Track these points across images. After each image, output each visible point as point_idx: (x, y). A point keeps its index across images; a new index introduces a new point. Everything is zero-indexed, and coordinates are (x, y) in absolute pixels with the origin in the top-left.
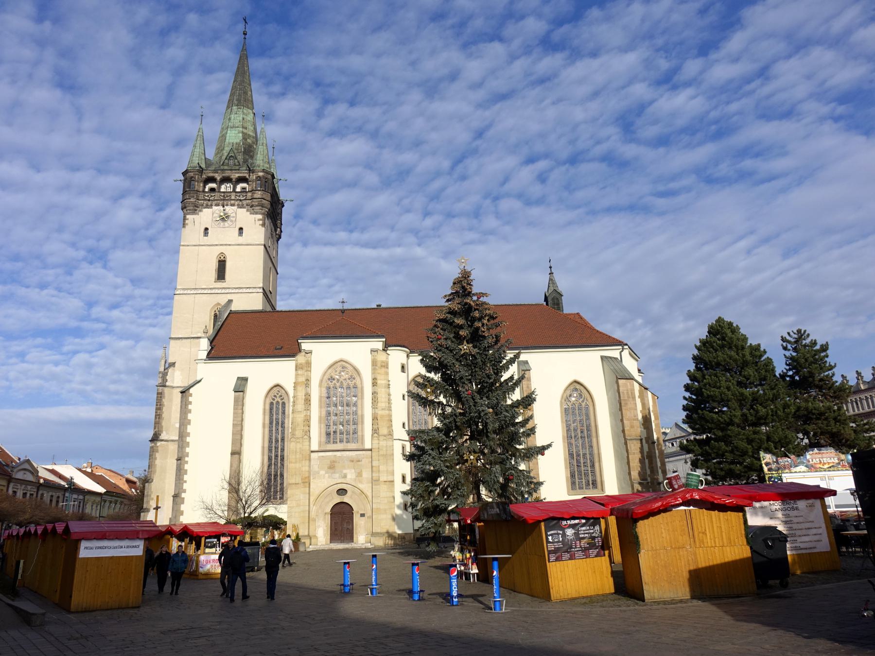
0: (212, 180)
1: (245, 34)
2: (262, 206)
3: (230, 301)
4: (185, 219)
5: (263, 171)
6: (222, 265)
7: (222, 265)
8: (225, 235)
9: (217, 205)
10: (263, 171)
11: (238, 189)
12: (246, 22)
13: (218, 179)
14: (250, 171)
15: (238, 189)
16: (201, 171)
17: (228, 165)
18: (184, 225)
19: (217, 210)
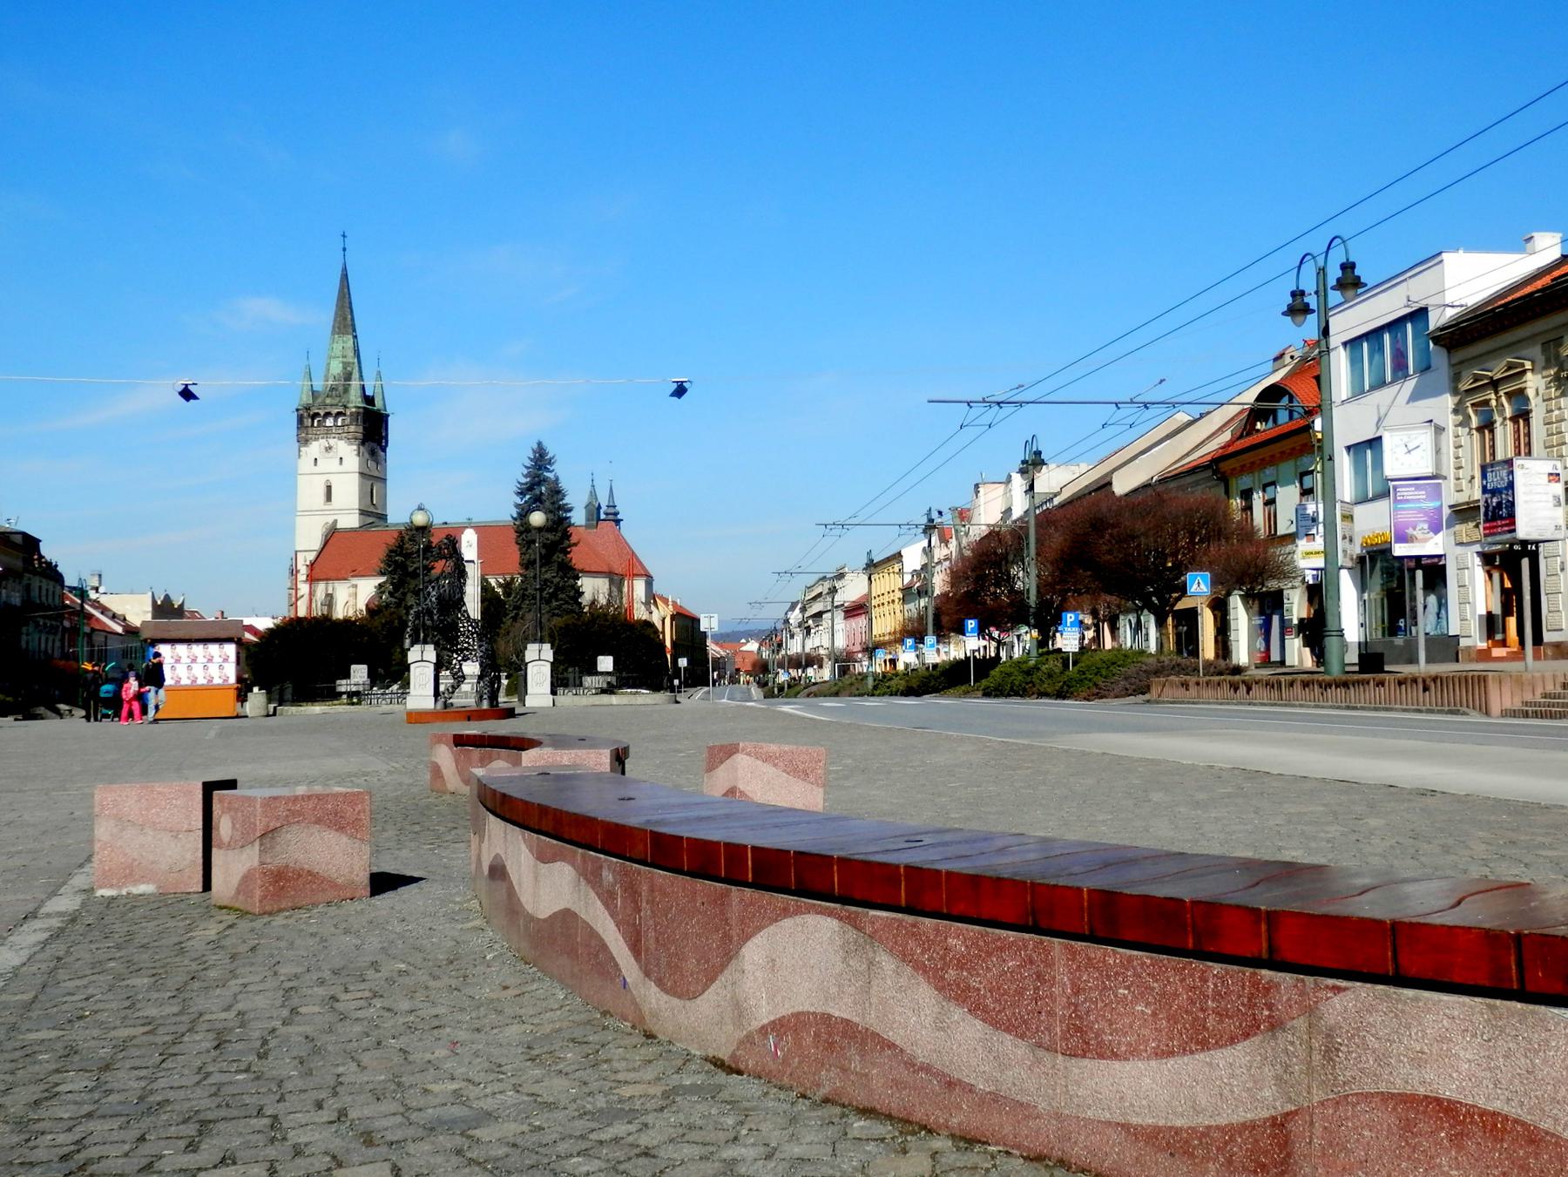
0: (317, 415)
1: (344, 249)
2: (356, 439)
3: (336, 521)
4: (300, 451)
5: (356, 407)
6: (329, 488)
7: (329, 488)
8: (328, 464)
9: (323, 438)
10: (356, 407)
11: (339, 424)
12: (344, 236)
13: (322, 414)
14: (345, 407)
15: (339, 424)
16: (307, 409)
17: (331, 396)
18: (299, 456)
19: (323, 442)
